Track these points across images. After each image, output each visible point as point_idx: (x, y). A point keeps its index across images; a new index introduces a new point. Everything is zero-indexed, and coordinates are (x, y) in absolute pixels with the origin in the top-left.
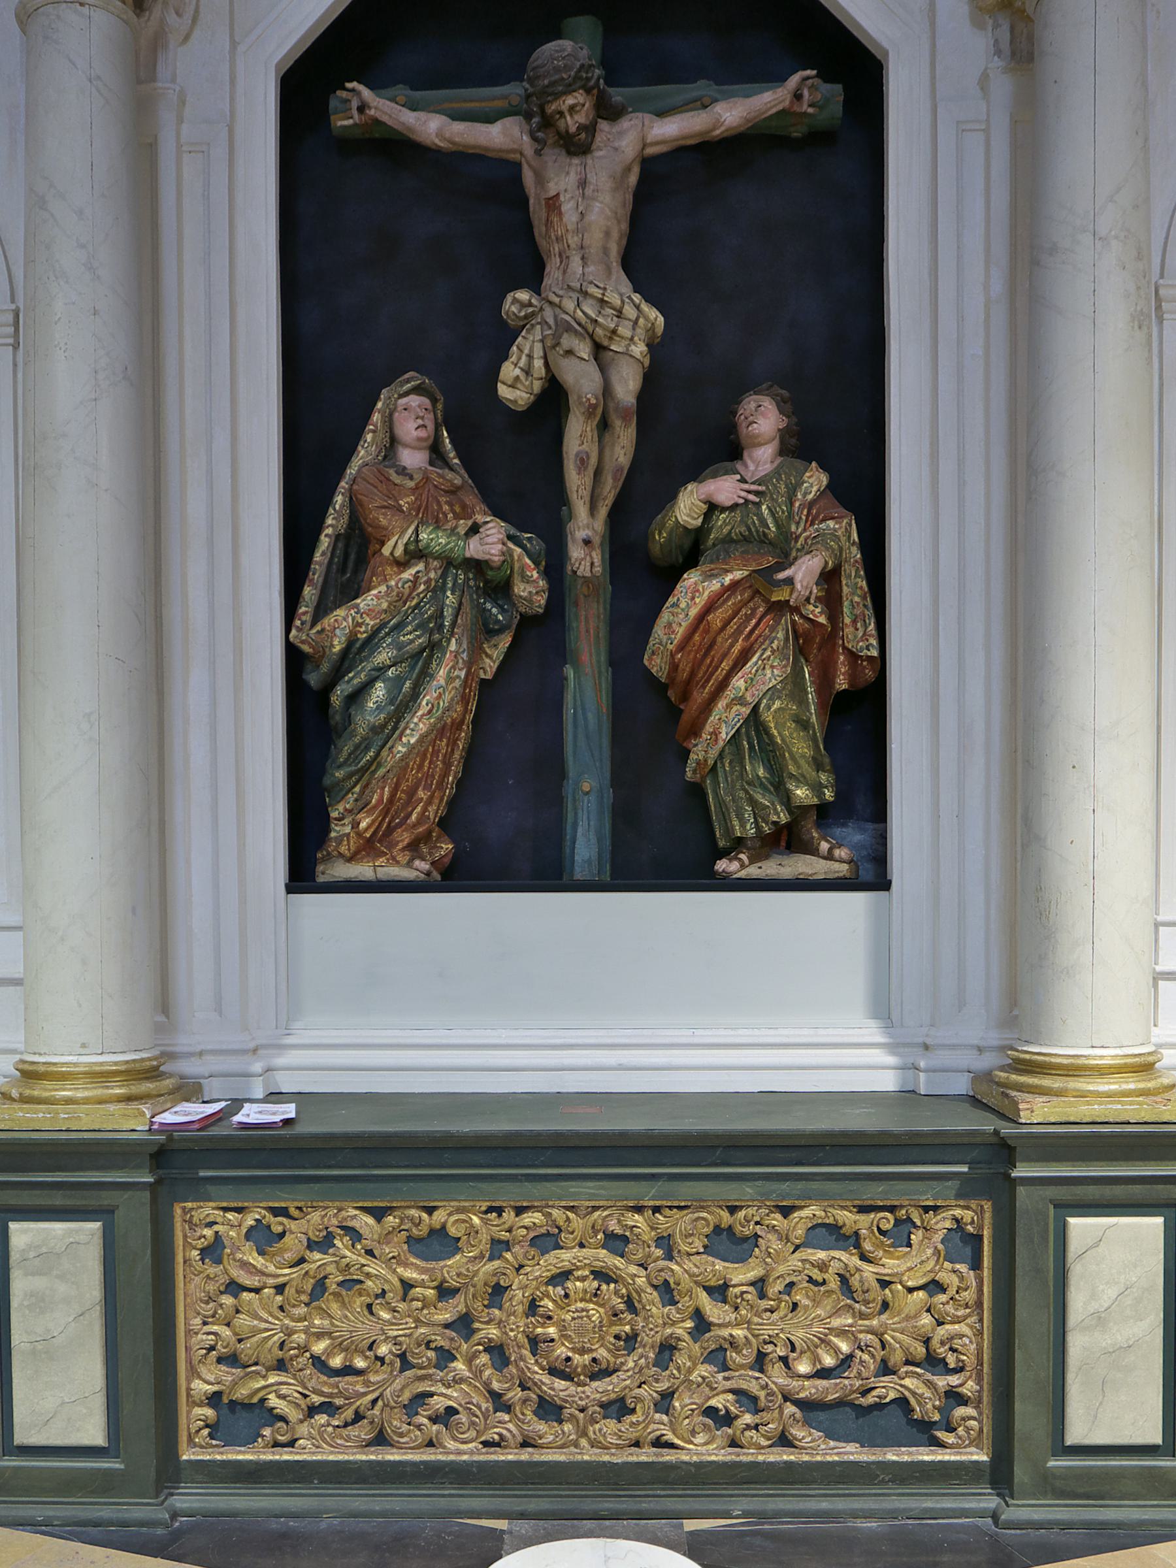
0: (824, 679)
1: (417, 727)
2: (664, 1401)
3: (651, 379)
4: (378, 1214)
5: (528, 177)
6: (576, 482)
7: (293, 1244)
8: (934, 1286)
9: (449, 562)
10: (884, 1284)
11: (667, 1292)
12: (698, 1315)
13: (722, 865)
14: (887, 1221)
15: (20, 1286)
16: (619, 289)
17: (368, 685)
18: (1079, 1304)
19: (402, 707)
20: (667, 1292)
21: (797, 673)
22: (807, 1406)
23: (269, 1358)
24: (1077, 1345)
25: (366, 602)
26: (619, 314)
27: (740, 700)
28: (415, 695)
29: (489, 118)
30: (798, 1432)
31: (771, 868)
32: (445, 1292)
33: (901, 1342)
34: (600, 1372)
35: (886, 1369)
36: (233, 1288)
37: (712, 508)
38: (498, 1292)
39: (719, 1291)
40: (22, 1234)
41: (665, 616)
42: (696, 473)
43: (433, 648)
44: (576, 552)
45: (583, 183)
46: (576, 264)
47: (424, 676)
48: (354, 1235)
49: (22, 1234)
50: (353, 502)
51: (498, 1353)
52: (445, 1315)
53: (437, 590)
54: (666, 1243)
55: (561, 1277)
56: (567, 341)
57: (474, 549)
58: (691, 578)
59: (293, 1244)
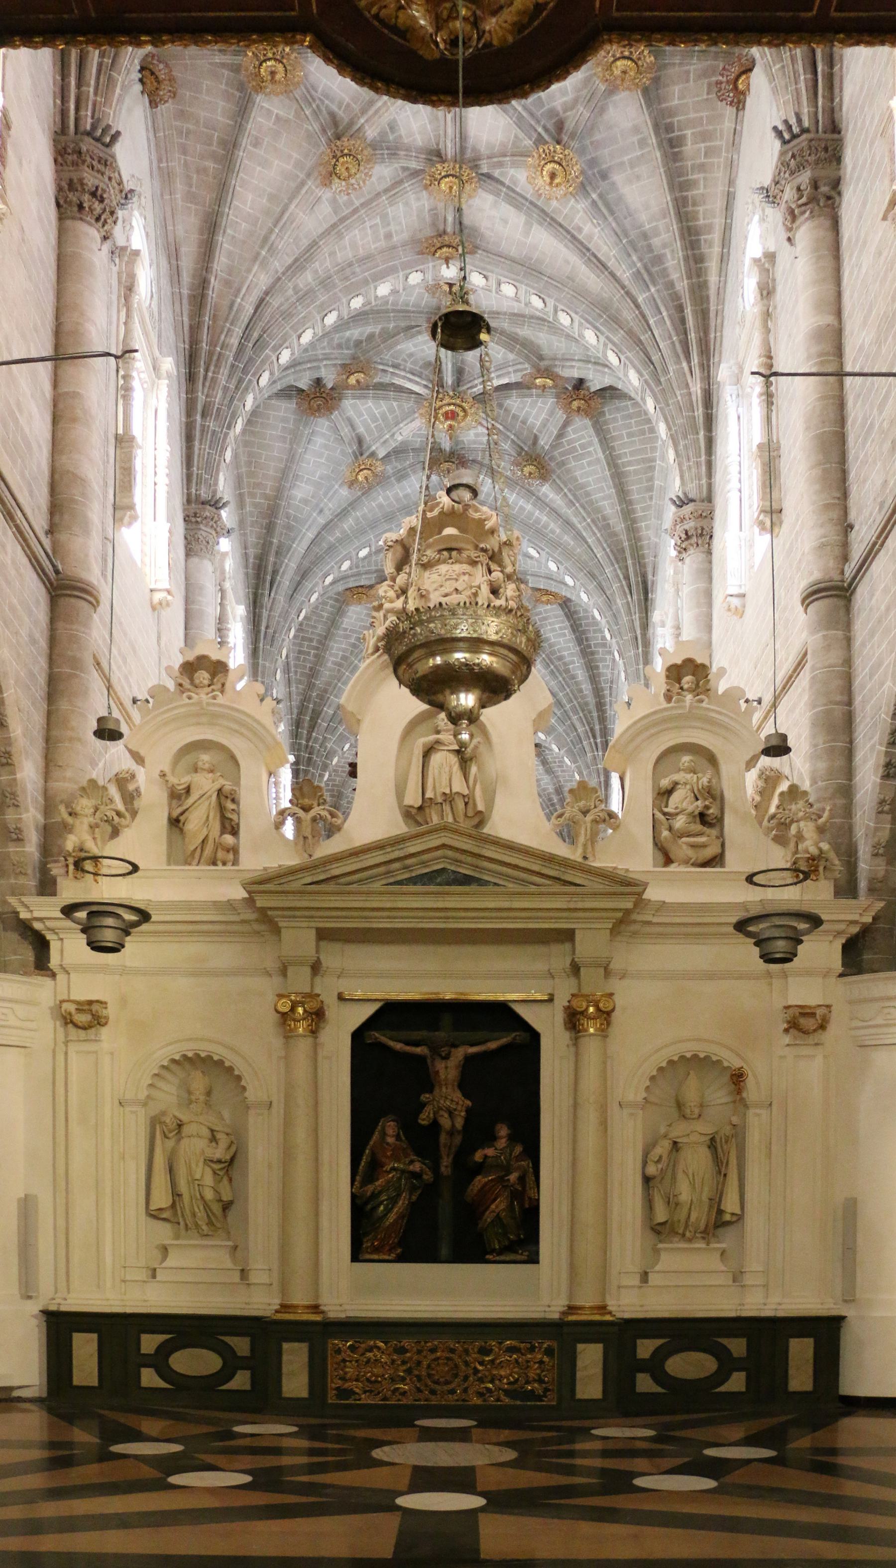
0: (521, 1205)
1: (392, 1217)
2: (465, 1390)
3: (467, 1120)
4: (386, 1343)
5: (429, 1061)
6: (443, 1151)
7: (361, 1351)
8: (541, 1362)
9: (403, 1172)
10: (528, 1362)
11: (467, 1364)
12: (475, 1368)
13: (488, 1257)
14: (529, 1345)
15: (285, 1358)
16: (458, 1095)
17: (379, 1206)
18: (580, 1364)
19: (388, 1211)
20: (467, 1364)
21: (512, 1203)
22: (506, 1391)
23: (354, 1377)
24: (579, 1375)
25: (377, 1183)
26: (457, 1103)
27: (493, 1211)
28: (392, 1208)
29: (417, 1044)
30: (502, 1397)
31: (502, 1258)
32: (404, 1363)
33: (532, 1375)
34: (447, 1383)
35: (528, 1382)
36: (344, 1361)
37: (486, 1157)
38: (419, 1363)
39: (481, 1363)
40: (285, 1346)
41: (471, 1187)
42: (482, 1146)
43: (399, 1195)
44: (443, 1169)
45: (446, 1068)
46: (444, 1090)
47: (396, 1202)
48: (379, 1348)
49: (285, 1346)
50: (373, 1154)
51: (419, 1378)
52: (404, 1368)
53: (400, 1179)
54: (466, 1352)
55: (438, 1359)
56: (442, 1113)
57: (411, 1168)
58: (479, 1178)
59: (361, 1351)
